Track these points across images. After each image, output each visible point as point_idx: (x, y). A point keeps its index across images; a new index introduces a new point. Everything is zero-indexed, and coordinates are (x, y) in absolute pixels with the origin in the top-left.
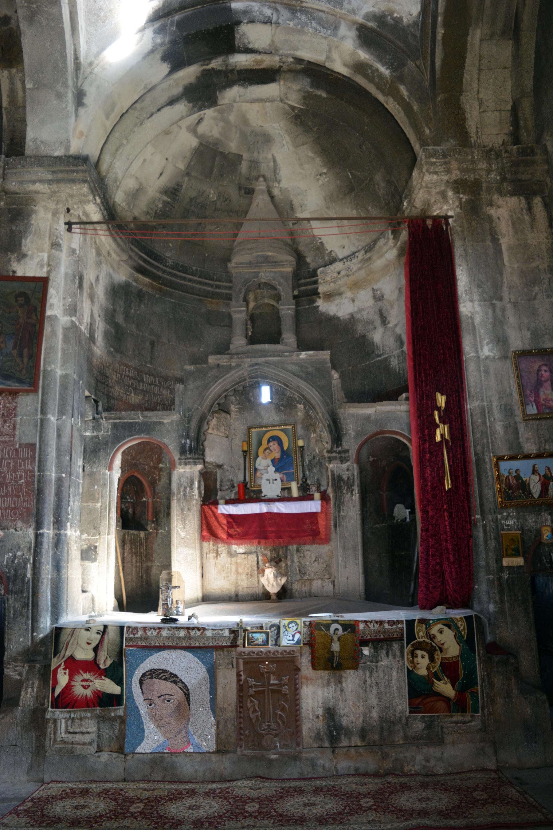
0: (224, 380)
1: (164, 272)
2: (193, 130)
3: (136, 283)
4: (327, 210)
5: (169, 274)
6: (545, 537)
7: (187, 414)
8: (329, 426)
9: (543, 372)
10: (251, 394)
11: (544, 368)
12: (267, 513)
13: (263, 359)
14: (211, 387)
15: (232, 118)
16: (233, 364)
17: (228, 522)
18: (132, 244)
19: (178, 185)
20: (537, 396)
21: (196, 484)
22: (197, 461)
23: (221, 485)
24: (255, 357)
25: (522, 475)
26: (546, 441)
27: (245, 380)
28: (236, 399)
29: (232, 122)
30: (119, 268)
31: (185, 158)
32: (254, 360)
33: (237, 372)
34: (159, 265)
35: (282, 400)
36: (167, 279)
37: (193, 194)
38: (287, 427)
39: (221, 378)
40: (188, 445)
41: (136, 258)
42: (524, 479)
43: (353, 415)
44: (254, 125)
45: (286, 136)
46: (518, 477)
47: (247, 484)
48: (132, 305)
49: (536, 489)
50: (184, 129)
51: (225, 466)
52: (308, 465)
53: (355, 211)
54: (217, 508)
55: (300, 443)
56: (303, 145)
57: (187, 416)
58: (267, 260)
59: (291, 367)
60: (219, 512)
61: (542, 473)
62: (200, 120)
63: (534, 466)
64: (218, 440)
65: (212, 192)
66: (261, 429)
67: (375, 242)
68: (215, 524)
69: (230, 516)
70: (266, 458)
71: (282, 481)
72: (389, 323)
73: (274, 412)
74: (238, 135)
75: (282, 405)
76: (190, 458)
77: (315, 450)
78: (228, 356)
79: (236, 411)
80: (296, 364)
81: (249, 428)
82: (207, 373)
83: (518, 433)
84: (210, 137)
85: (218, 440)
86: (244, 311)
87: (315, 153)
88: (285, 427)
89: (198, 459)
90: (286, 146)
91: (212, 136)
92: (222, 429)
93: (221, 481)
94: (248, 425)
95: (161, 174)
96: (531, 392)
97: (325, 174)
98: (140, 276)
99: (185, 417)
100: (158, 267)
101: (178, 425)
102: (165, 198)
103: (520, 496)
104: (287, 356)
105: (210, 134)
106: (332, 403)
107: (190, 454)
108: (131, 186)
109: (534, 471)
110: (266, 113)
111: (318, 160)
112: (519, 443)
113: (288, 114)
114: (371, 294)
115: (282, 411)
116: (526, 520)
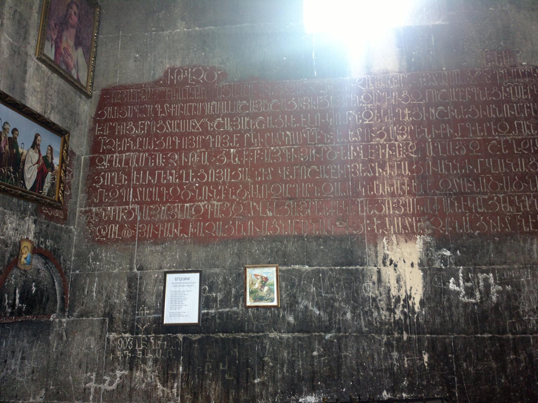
6: (23, 260)
9: (73, 13)
11: (75, 7)
20: (60, 37)
25: (19, 141)
26: (53, 108)
42: (21, 150)
46: (13, 142)
49: (31, 175)
61: (43, 154)
63: (36, 137)
83: (25, 72)
96: (55, 26)
103: (8, 177)
109: (35, 145)
112: (23, 89)
116: (5, 223)
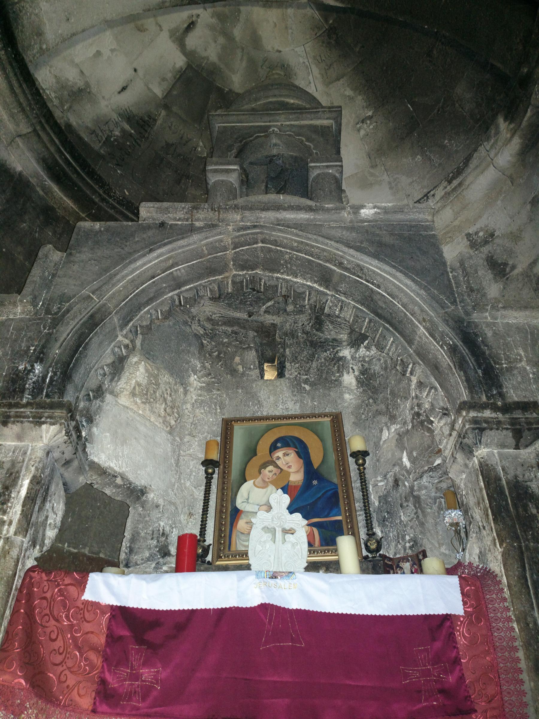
0: (173, 250)
1: (103, 200)
2: (180, 37)
3: (46, 194)
4: (372, 171)
5: (114, 207)
7: (55, 309)
8: (453, 350)
10: (237, 359)
12: (264, 607)
13: (271, 215)
14: (135, 260)
15: (237, 32)
16: (197, 224)
17: (112, 639)
18: (47, 122)
19: (149, 117)
21: (24, 487)
22: (47, 413)
23: (131, 550)
24: (251, 209)
27: (224, 269)
28: (204, 367)
29: (237, 39)
30: (10, 144)
31: (164, 79)
32: (251, 217)
33: (206, 238)
34: (96, 187)
35: (307, 372)
36: (106, 212)
37: (172, 138)
38: (320, 420)
39: (165, 244)
40: (33, 378)
41: (52, 149)
43: (519, 329)
44: (269, 48)
45: (314, 67)
47: (206, 551)
48: (26, 217)
50: (165, 35)
51: (151, 496)
52: (379, 510)
53: (419, 157)
54: (82, 585)
55: (357, 444)
56: (338, 79)
57: (55, 309)
58: (284, 106)
59: (338, 233)
60: (87, 596)
62: (191, 26)
64: (142, 428)
65: (201, 144)
66: (257, 424)
67: (467, 160)
68: (54, 646)
69: (123, 615)
70: (265, 485)
71: (310, 544)
72: (514, 267)
73: (287, 394)
74: (244, 64)
75: (306, 382)
76: (28, 404)
77: (399, 462)
78: (188, 205)
79: (201, 388)
80: (352, 229)
81: (228, 426)
82: (132, 235)
84: (203, 58)
85: (142, 428)
86: (235, 170)
87: (354, 89)
88: (314, 420)
89: (52, 406)
90: (312, 85)
91: (207, 58)
92: (161, 408)
93: (133, 540)
94: (226, 416)
95: (124, 89)
97: (370, 118)
98: (55, 188)
99: (48, 312)
100: (92, 186)
101: (19, 330)
102: (127, 127)
104: (328, 210)
105: (204, 54)
106: (454, 302)
107: (34, 396)
108: (71, 79)
110: (286, 28)
111: (360, 100)
113: (319, 28)
114: (466, 243)
115: (308, 393)
